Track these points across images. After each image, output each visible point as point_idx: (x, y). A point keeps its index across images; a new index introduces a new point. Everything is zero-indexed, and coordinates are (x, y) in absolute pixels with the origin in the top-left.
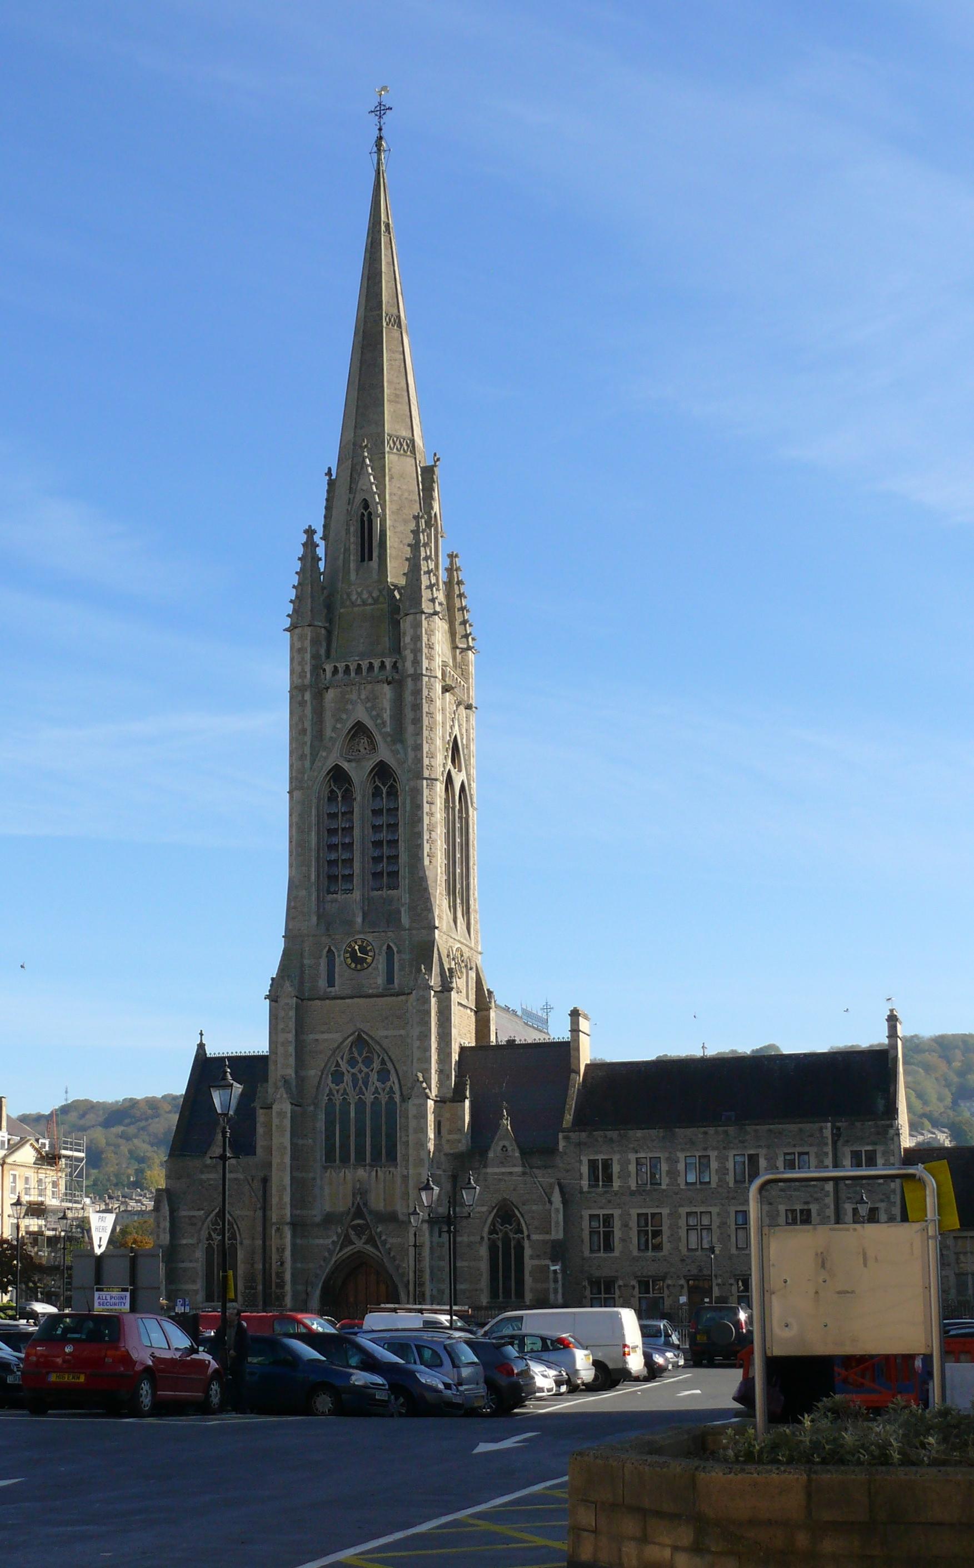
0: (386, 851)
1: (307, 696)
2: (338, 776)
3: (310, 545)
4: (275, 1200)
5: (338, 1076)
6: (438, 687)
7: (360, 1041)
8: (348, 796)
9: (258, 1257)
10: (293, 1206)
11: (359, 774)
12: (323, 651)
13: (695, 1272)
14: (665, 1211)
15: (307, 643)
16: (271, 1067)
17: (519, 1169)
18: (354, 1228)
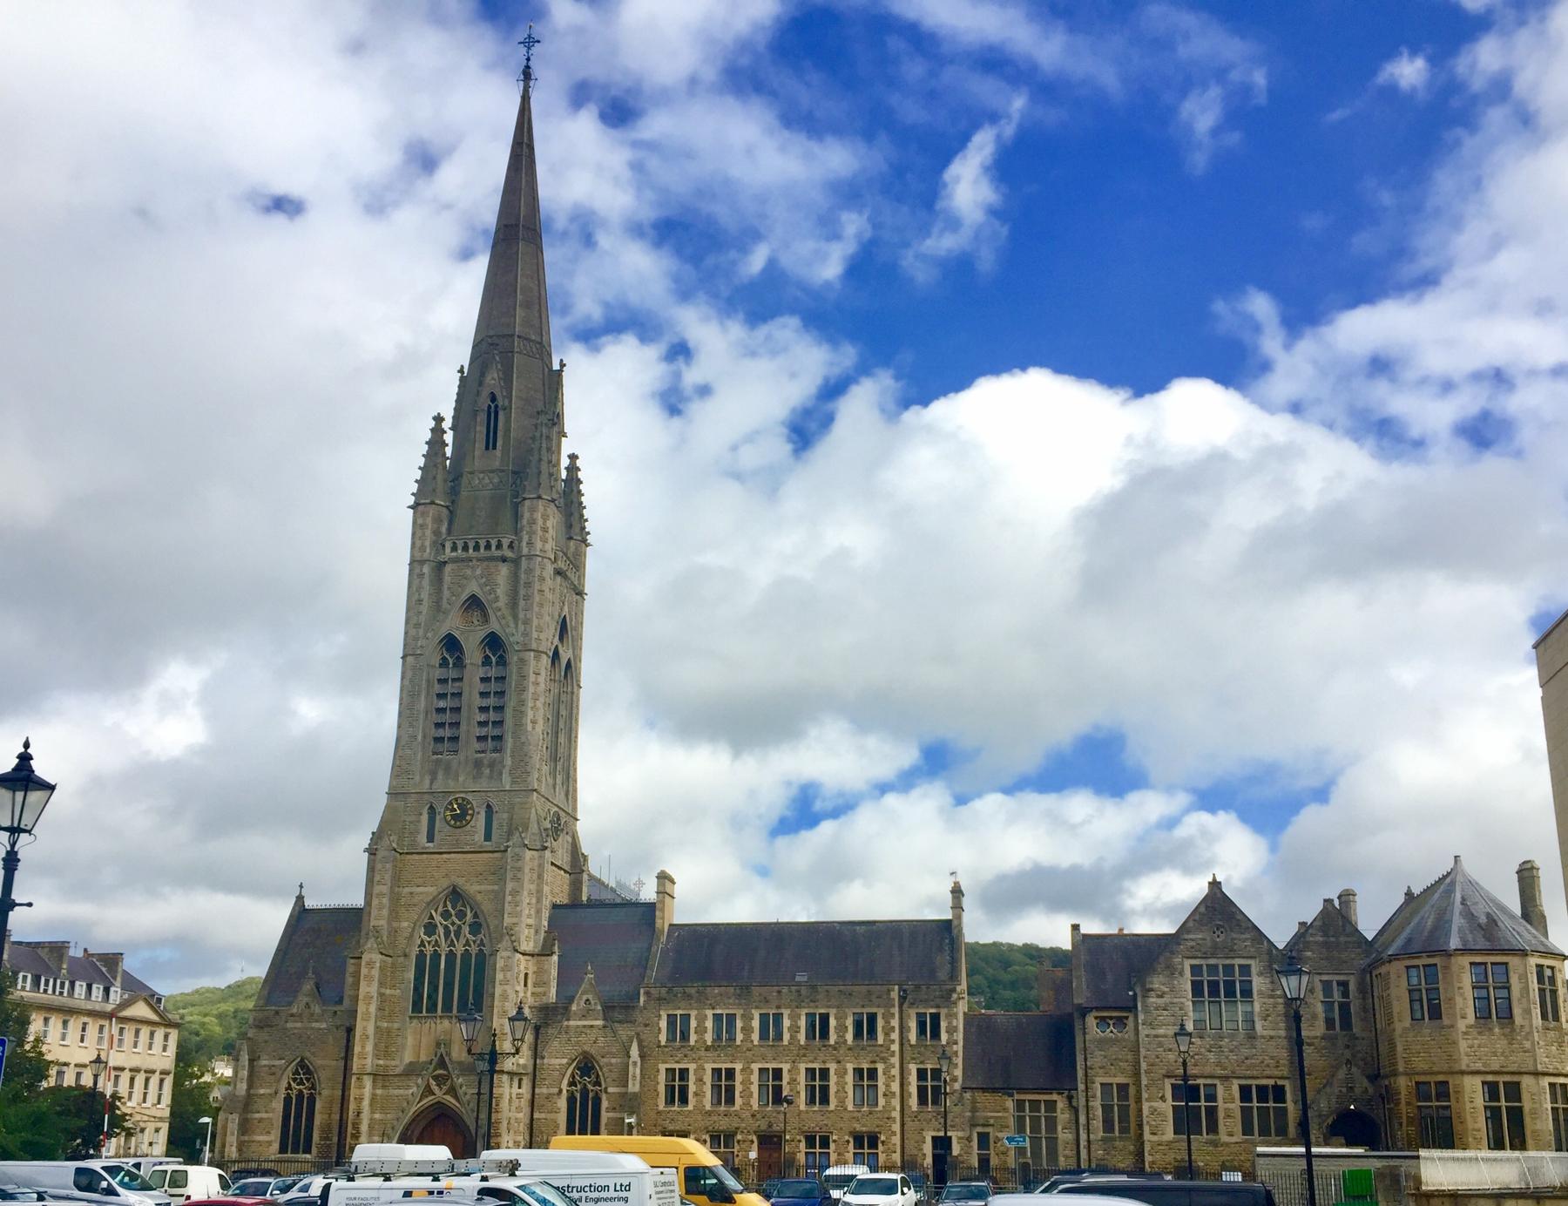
0: (492, 716)
1: (426, 569)
3: (438, 431)
4: (357, 1049)
5: (430, 929)
6: (550, 569)
7: (455, 894)
8: (459, 663)
9: (336, 1108)
10: (377, 1057)
12: (444, 529)
13: (764, 1127)
14: (738, 1067)
15: (429, 520)
16: (365, 918)
17: (600, 1023)
18: (436, 1078)
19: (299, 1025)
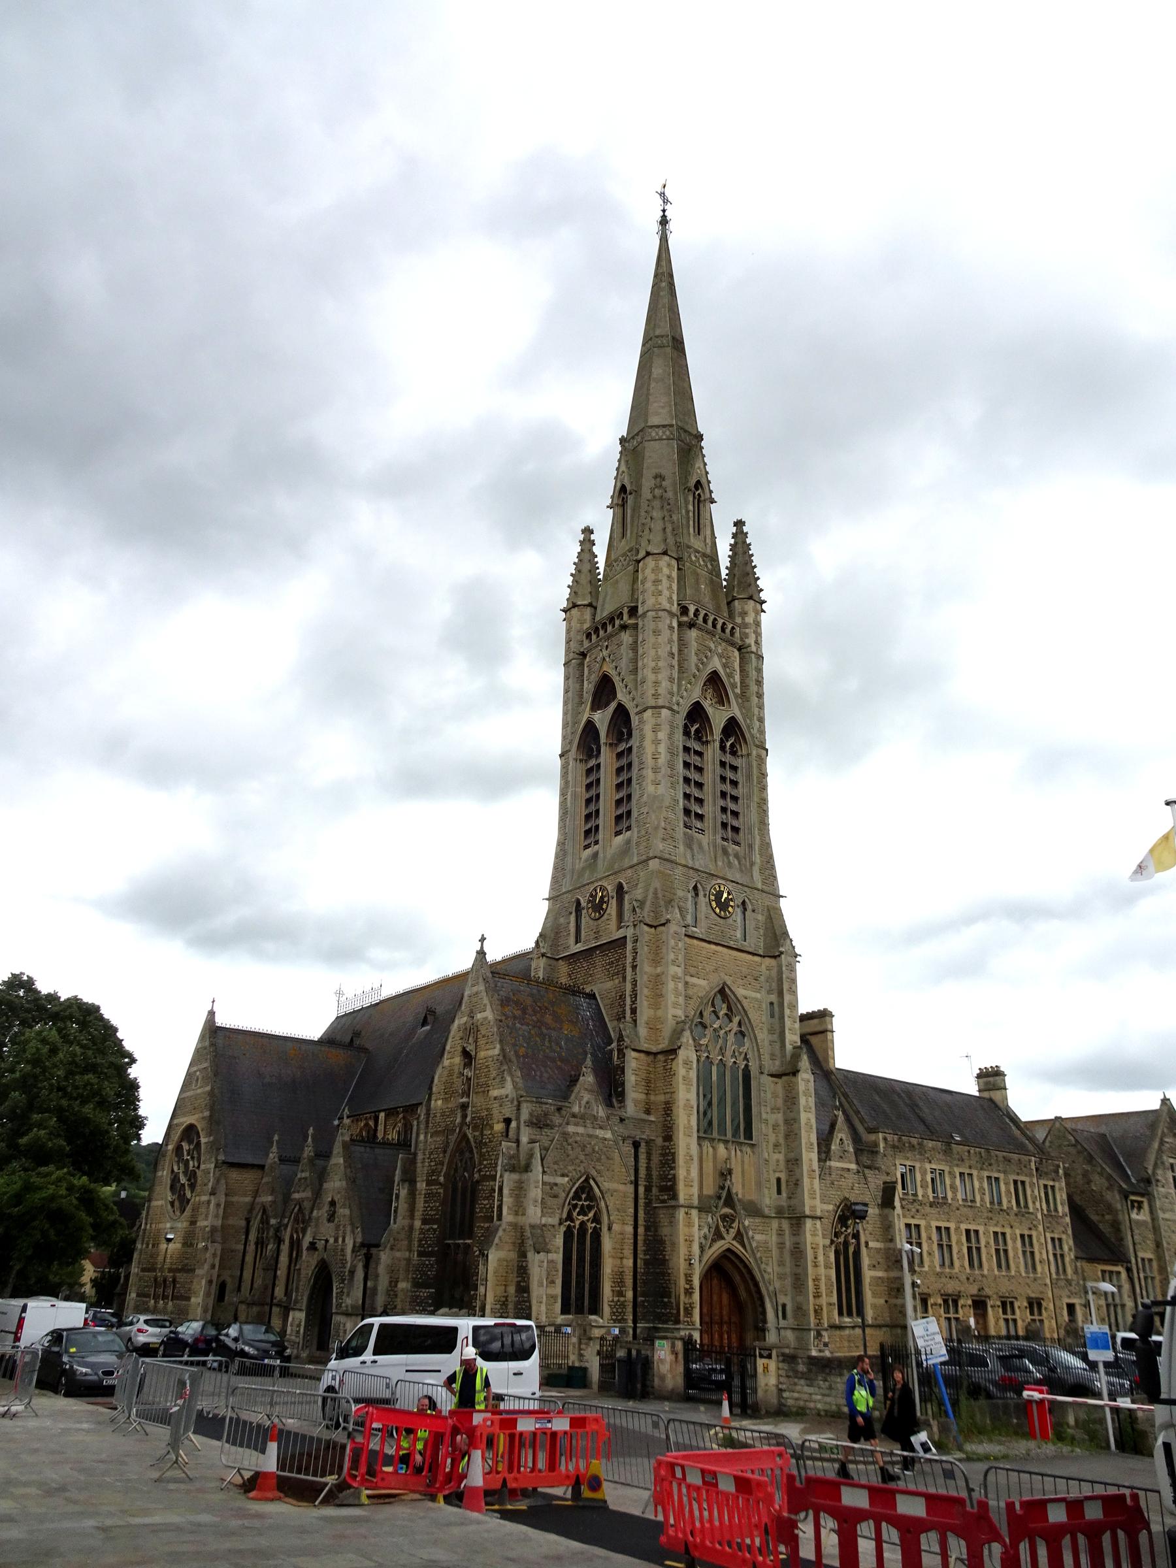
2: (697, 713)
7: (722, 992)
9: (628, 1252)
11: (718, 718)
13: (975, 1292)
19: (581, 1130)
